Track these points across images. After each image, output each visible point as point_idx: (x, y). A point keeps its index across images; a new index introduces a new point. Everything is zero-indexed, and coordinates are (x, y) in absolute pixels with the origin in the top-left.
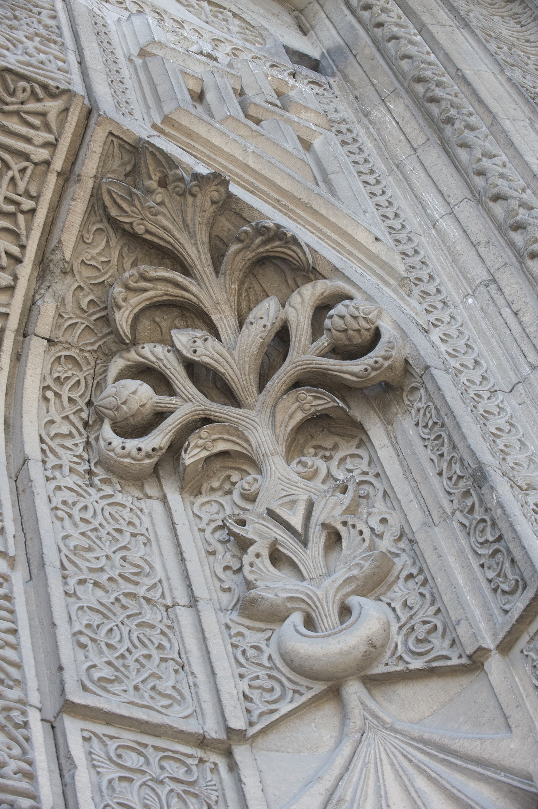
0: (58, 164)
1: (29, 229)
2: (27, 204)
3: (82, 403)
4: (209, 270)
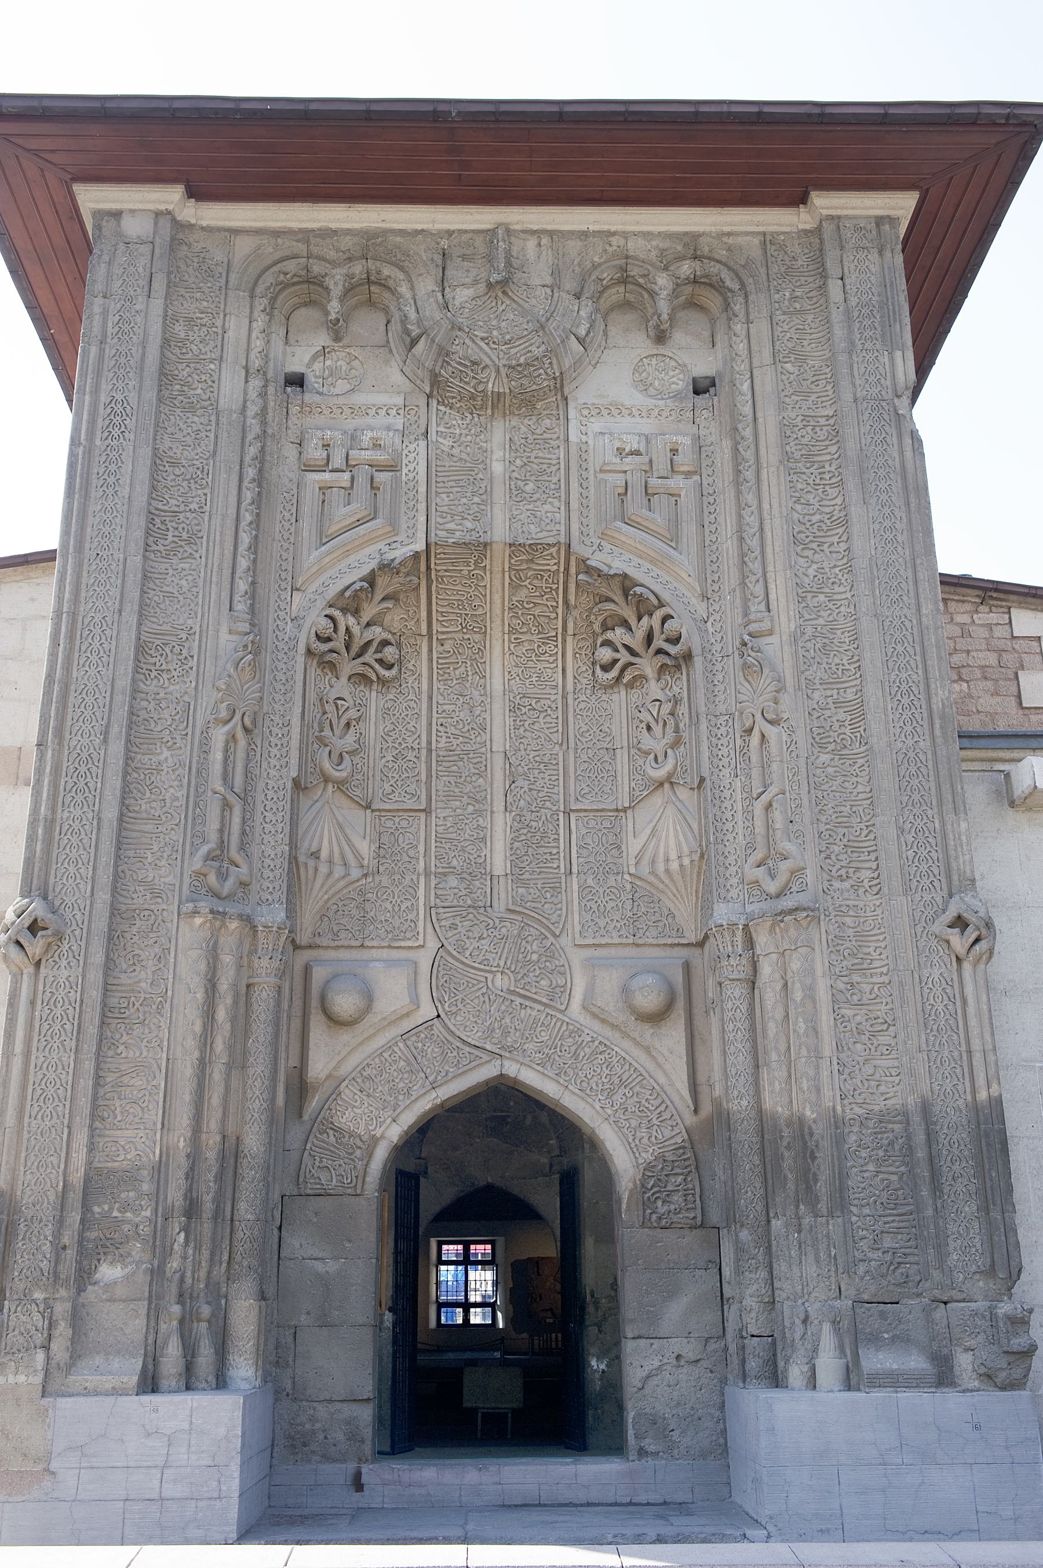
0: (562, 569)
1: (557, 594)
2: (555, 586)
3: (590, 655)
4: (624, 604)
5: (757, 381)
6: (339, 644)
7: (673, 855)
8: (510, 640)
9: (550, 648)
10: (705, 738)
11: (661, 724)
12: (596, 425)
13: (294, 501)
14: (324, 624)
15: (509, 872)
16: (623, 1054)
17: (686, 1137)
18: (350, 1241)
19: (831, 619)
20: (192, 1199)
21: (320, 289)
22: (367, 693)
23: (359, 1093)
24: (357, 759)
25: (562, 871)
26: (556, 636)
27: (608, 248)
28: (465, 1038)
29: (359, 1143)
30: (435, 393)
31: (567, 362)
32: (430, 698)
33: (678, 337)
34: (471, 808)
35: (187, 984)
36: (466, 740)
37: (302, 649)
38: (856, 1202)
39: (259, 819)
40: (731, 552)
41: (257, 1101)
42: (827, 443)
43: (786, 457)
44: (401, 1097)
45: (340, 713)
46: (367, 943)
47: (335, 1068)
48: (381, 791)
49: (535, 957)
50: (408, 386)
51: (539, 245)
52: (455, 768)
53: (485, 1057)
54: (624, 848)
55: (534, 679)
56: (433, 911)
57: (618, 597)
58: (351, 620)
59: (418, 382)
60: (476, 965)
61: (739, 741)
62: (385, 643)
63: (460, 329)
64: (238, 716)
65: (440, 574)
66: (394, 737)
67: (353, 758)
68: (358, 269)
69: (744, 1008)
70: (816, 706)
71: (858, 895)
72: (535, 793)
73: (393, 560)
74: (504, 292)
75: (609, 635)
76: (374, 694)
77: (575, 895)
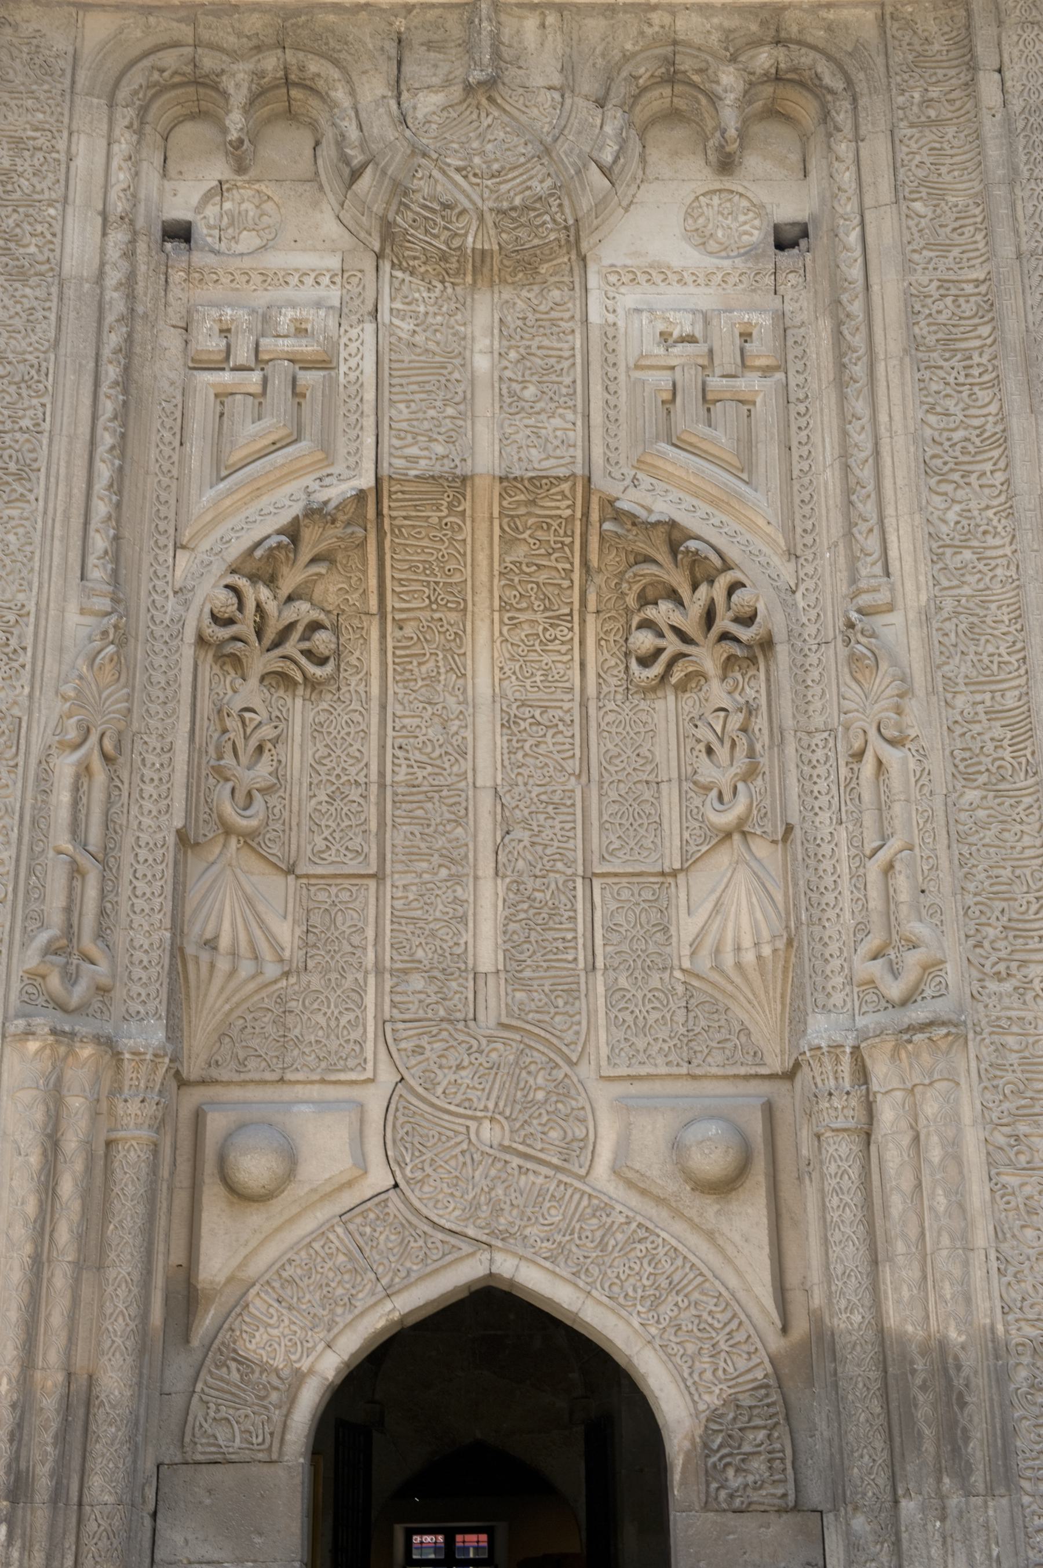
0: (579, 515)
1: (572, 552)
2: (568, 540)
3: (622, 642)
4: (671, 566)
5: (870, 230)
6: (245, 628)
7: (747, 942)
8: (502, 622)
9: (561, 631)
10: (792, 767)
11: (728, 744)
12: (629, 298)
13: (178, 414)
14: (224, 600)
15: (501, 967)
16: (674, 1242)
17: (770, 1369)
18: (260, 1534)
19: (981, 586)
20: (18, 1473)
21: (214, 94)
22: (289, 701)
23: (276, 1305)
24: (273, 800)
25: (581, 965)
26: (571, 614)
27: (646, 28)
28: (436, 1219)
29: (276, 1382)
30: (388, 251)
31: (585, 203)
32: (383, 707)
33: (753, 163)
34: (444, 873)
35: (15, 1142)
36: (437, 770)
37: (190, 635)
38: (1029, 1473)
39: (125, 891)
40: (831, 487)
41: (120, 1320)
42: (976, 321)
43: (915, 343)
44: (339, 1310)
45: (249, 730)
46: (289, 1076)
47: (242, 1265)
48: (309, 848)
49: (540, 1095)
50: (346, 241)
51: (543, 26)
52: (420, 813)
53: (466, 1248)
54: (673, 930)
55: (538, 679)
56: (388, 1027)
57: (662, 555)
58: (264, 593)
59: (363, 235)
60: (452, 1108)
61: (843, 771)
62: (315, 626)
63: (425, 155)
64: (94, 738)
65: (397, 522)
66: (330, 765)
67: (267, 798)
68: (271, 62)
69: (854, 1173)
70: (959, 718)
71: (1024, 1003)
72: (539, 849)
73: (326, 503)
74: (491, 99)
75: (650, 612)
76: (299, 702)
77: (601, 1001)
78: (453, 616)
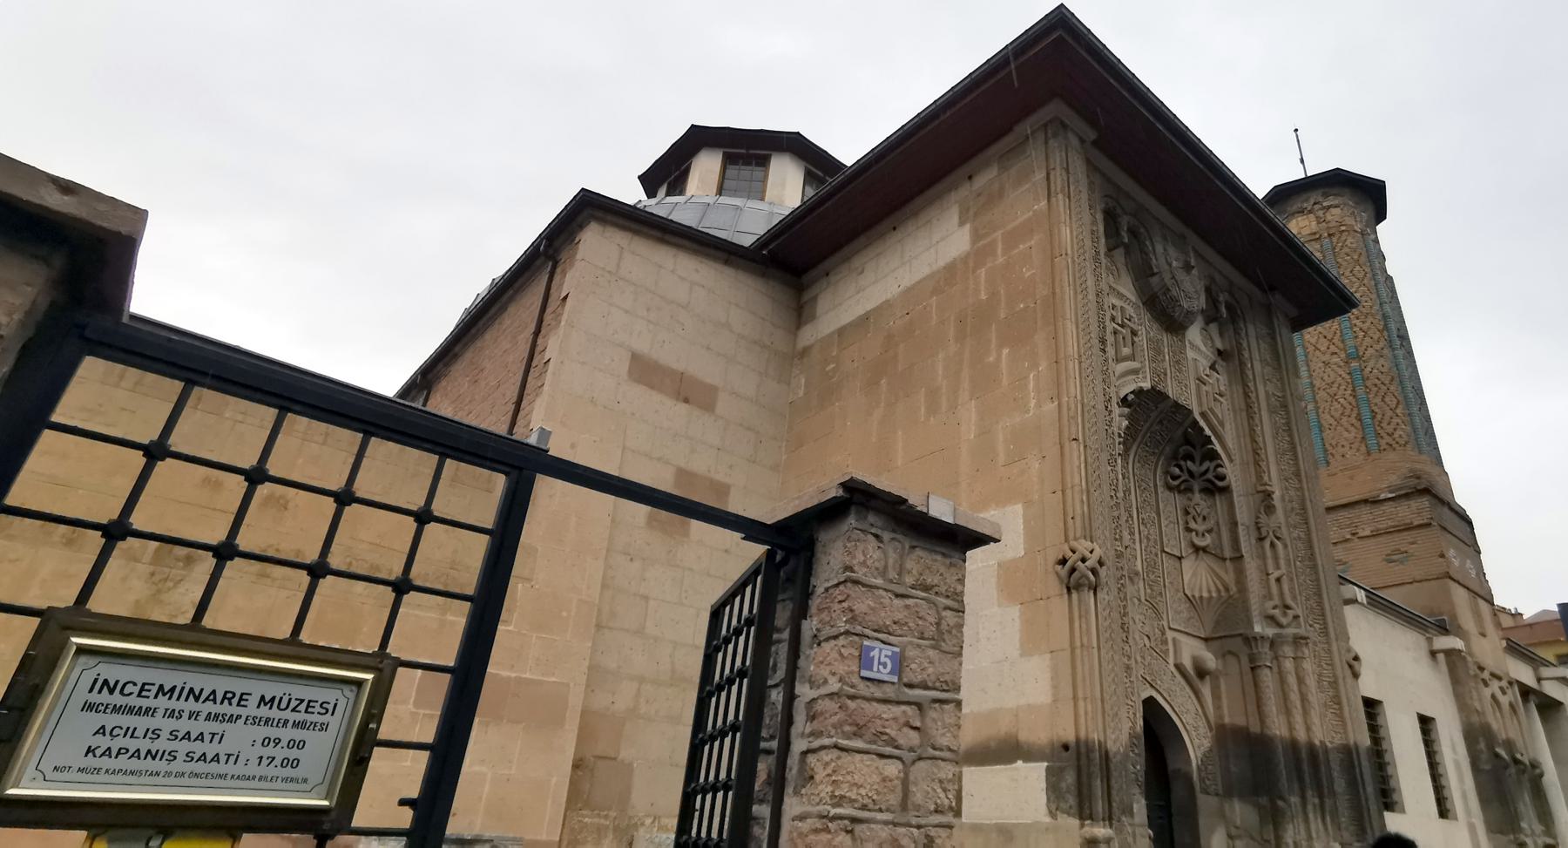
75: (1182, 463)
78: (1131, 440)
